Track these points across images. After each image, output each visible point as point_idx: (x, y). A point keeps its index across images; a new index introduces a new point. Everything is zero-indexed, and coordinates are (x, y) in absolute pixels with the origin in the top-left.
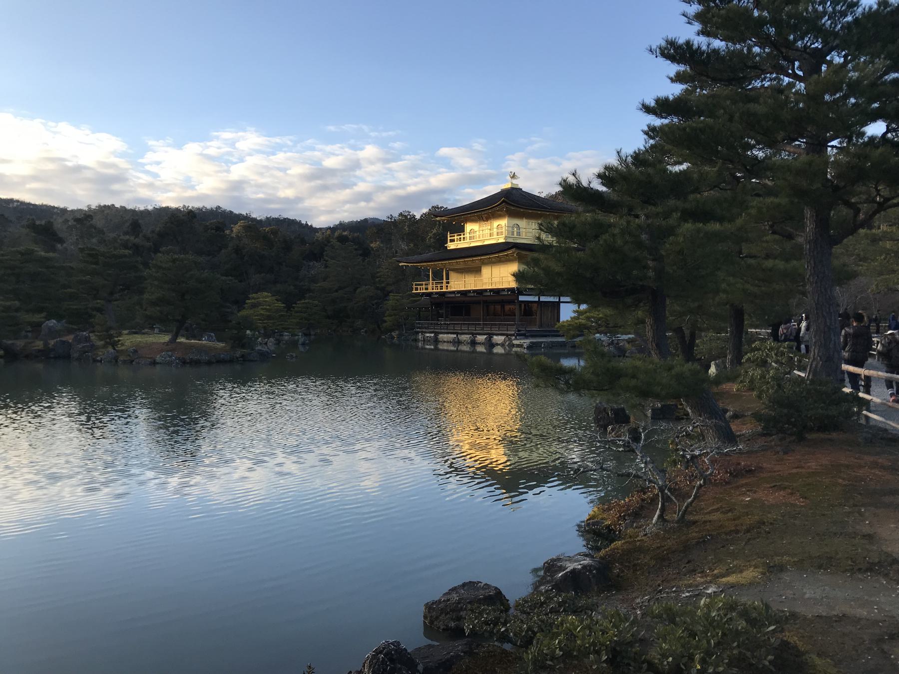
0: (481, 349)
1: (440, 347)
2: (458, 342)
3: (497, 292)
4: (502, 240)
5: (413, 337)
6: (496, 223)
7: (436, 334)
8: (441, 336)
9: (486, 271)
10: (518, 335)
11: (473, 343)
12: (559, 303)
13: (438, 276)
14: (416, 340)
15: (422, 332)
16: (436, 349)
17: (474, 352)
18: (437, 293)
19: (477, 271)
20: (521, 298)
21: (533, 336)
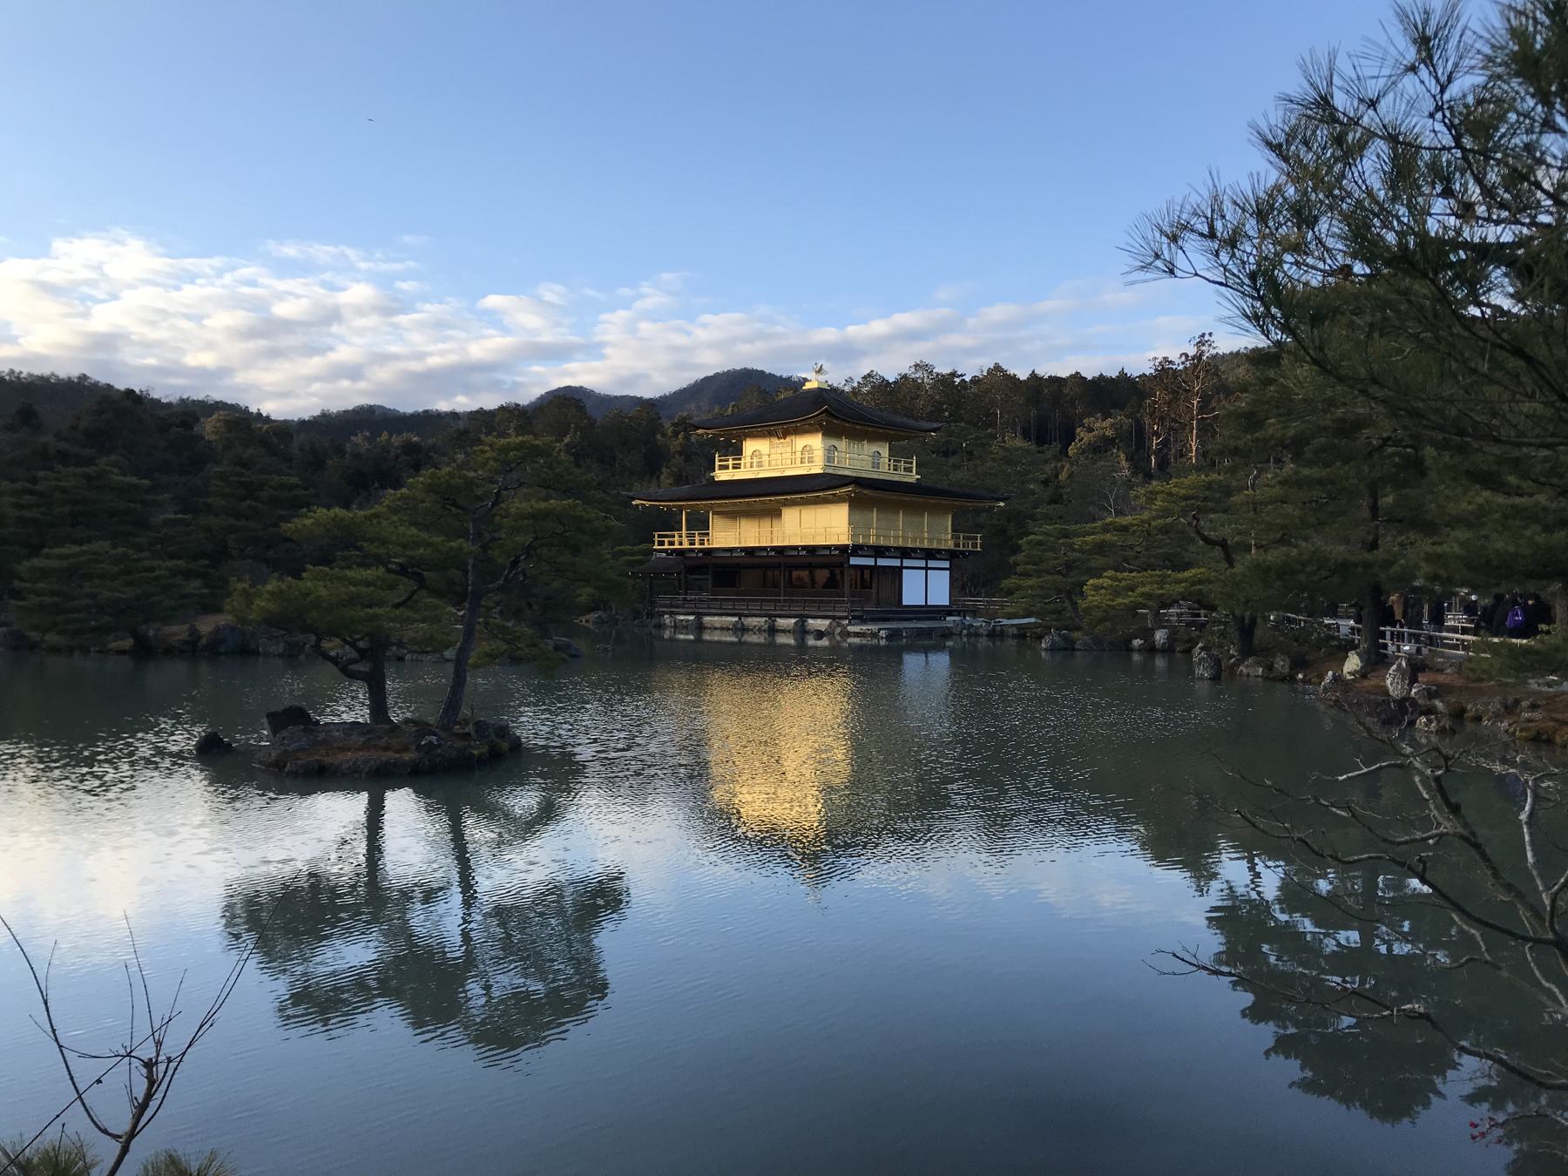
0: (782, 639)
1: (706, 637)
2: (742, 630)
3: (812, 550)
4: (817, 469)
6: (801, 442)
7: (699, 615)
8: (707, 619)
9: (790, 516)
10: (854, 618)
11: (773, 630)
12: (902, 568)
13: (700, 524)
14: (661, 626)
15: (672, 614)
16: (699, 640)
17: (772, 644)
18: (700, 550)
19: (775, 514)
20: (854, 561)
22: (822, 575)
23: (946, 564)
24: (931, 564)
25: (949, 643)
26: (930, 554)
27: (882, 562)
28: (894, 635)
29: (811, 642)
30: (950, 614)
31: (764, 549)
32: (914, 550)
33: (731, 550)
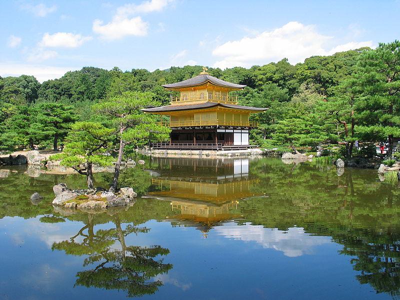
1: (169, 156)
3: (204, 127)
5: (152, 152)
8: (169, 151)
12: (233, 133)
15: (158, 149)
19: (191, 117)
20: (218, 131)
21: (225, 150)
22: (207, 136)
23: (247, 131)
24: (243, 131)
25: (250, 157)
26: (242, 129)
27: (227, 131)
28: (233, 155)
29: (204, 157)
30: (249, 148)
31: (189, 127)
32: (238, 127)
33: (177, 128)
